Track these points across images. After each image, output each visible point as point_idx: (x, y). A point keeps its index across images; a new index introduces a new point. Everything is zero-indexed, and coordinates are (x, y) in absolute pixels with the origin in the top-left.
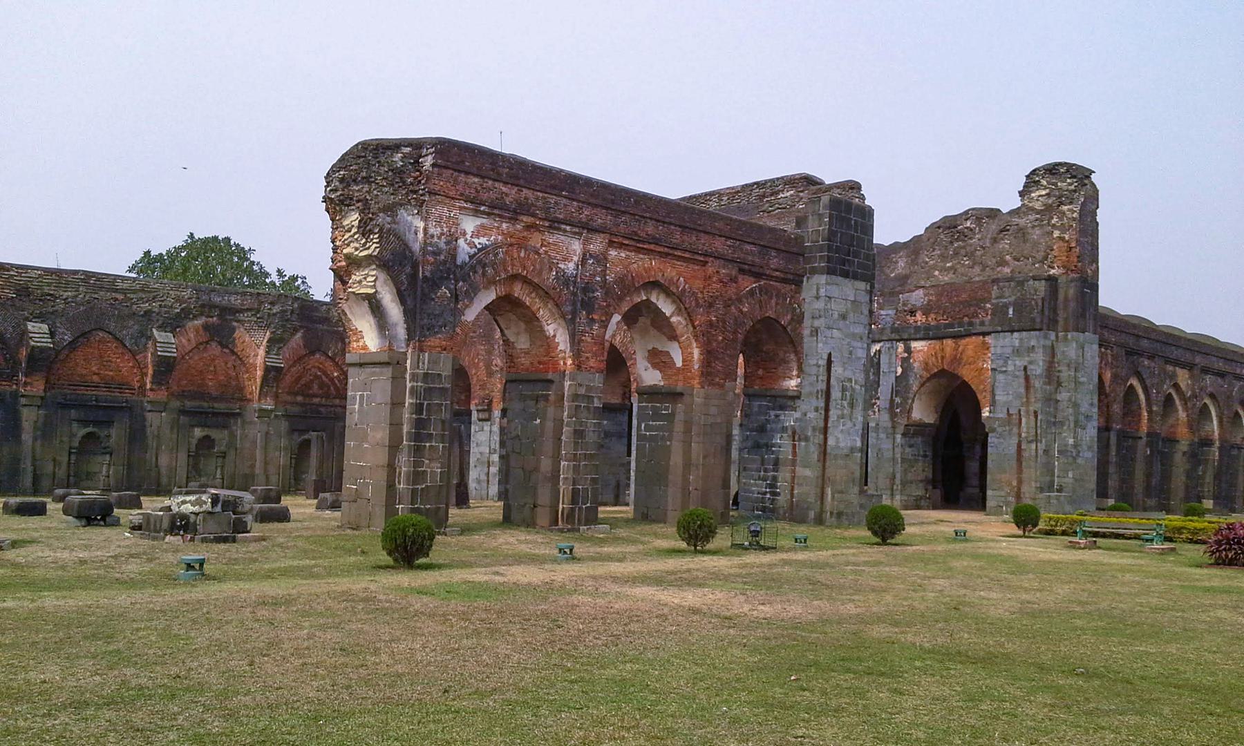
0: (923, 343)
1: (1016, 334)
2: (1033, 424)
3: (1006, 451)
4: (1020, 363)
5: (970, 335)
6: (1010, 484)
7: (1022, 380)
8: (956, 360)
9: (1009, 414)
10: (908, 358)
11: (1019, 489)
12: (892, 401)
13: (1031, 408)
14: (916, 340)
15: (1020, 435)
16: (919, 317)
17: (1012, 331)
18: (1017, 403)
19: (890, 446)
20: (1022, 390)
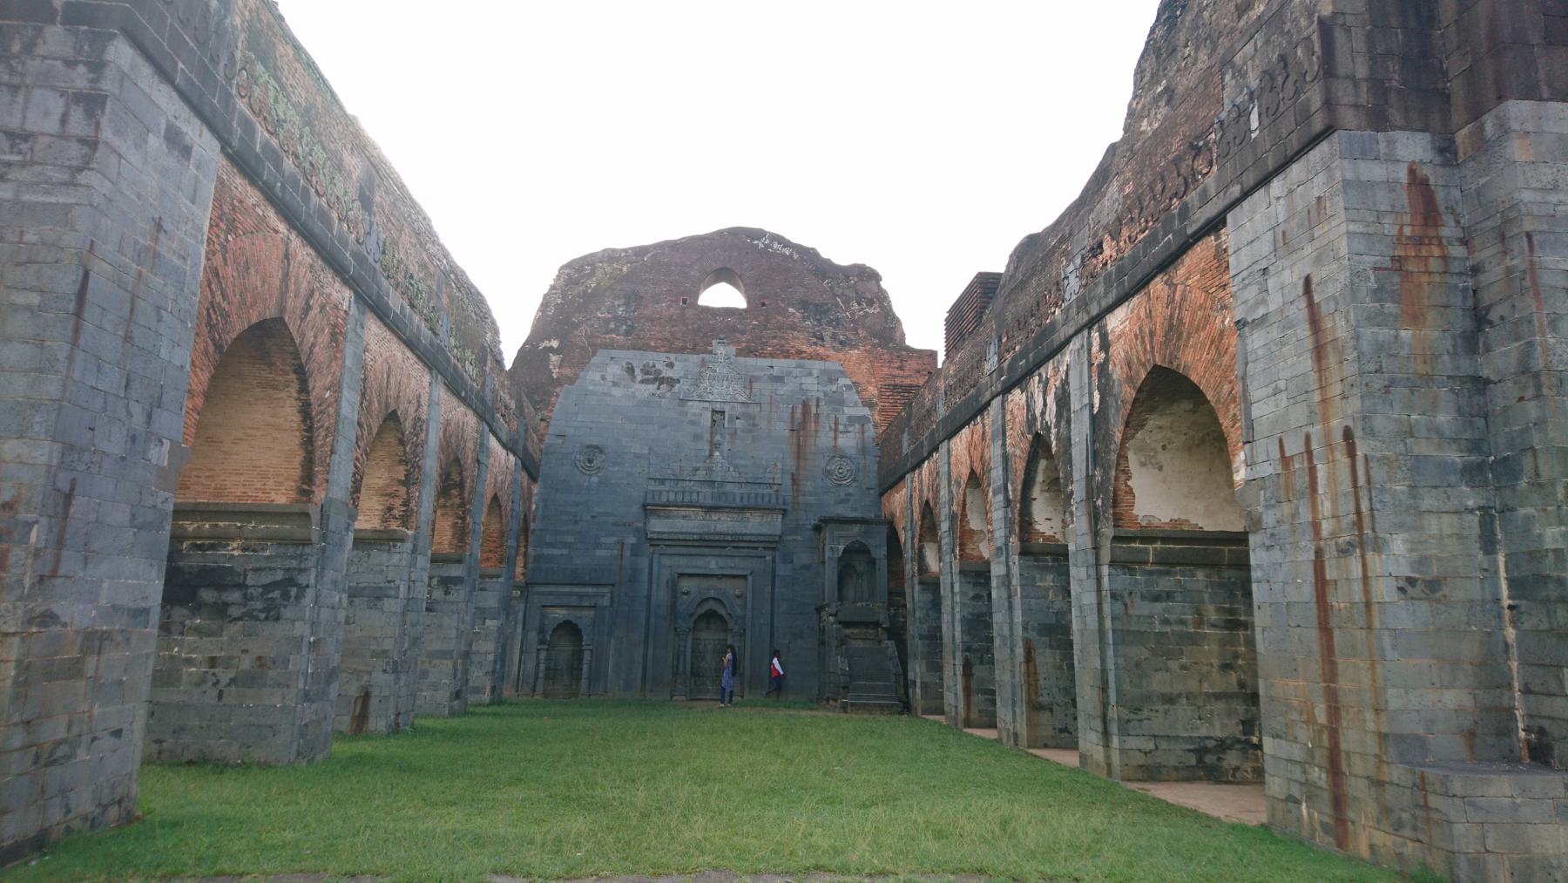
0: (1121, 313)
1: (1277, 186)
2: (1346, 486)
3: (1293, 596)
4: (1288, 277)
5: (1185, 247)
6: (1311, 720)
7: (1304, 331)
8: (1174, 331)
9: (1286, 461)
10: (1107, 360)
11: (1334, 734)
12: (1089, 478)
13: (1337, 424)
14: (1111, 309)
15: (1316, 526)
16: (1108, 250)
17: (1264, 181)
18: (1298, 415)
19: (1094, 601)
20: (1307, 363)
